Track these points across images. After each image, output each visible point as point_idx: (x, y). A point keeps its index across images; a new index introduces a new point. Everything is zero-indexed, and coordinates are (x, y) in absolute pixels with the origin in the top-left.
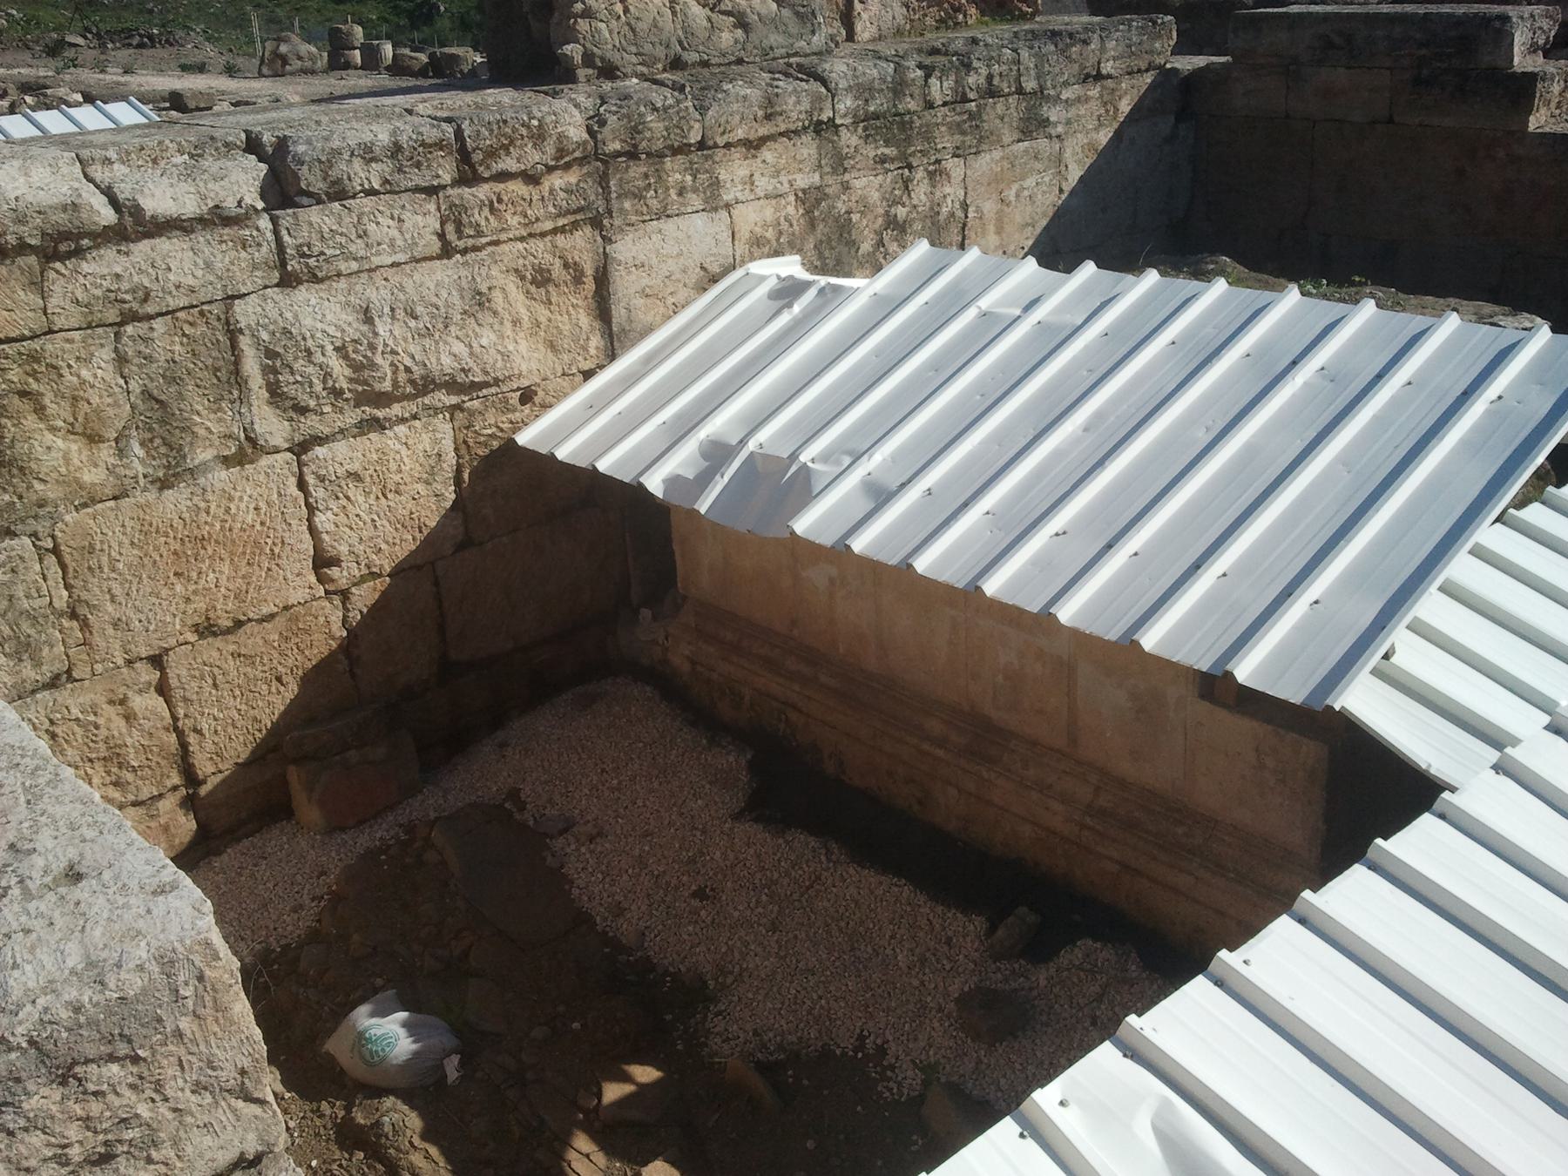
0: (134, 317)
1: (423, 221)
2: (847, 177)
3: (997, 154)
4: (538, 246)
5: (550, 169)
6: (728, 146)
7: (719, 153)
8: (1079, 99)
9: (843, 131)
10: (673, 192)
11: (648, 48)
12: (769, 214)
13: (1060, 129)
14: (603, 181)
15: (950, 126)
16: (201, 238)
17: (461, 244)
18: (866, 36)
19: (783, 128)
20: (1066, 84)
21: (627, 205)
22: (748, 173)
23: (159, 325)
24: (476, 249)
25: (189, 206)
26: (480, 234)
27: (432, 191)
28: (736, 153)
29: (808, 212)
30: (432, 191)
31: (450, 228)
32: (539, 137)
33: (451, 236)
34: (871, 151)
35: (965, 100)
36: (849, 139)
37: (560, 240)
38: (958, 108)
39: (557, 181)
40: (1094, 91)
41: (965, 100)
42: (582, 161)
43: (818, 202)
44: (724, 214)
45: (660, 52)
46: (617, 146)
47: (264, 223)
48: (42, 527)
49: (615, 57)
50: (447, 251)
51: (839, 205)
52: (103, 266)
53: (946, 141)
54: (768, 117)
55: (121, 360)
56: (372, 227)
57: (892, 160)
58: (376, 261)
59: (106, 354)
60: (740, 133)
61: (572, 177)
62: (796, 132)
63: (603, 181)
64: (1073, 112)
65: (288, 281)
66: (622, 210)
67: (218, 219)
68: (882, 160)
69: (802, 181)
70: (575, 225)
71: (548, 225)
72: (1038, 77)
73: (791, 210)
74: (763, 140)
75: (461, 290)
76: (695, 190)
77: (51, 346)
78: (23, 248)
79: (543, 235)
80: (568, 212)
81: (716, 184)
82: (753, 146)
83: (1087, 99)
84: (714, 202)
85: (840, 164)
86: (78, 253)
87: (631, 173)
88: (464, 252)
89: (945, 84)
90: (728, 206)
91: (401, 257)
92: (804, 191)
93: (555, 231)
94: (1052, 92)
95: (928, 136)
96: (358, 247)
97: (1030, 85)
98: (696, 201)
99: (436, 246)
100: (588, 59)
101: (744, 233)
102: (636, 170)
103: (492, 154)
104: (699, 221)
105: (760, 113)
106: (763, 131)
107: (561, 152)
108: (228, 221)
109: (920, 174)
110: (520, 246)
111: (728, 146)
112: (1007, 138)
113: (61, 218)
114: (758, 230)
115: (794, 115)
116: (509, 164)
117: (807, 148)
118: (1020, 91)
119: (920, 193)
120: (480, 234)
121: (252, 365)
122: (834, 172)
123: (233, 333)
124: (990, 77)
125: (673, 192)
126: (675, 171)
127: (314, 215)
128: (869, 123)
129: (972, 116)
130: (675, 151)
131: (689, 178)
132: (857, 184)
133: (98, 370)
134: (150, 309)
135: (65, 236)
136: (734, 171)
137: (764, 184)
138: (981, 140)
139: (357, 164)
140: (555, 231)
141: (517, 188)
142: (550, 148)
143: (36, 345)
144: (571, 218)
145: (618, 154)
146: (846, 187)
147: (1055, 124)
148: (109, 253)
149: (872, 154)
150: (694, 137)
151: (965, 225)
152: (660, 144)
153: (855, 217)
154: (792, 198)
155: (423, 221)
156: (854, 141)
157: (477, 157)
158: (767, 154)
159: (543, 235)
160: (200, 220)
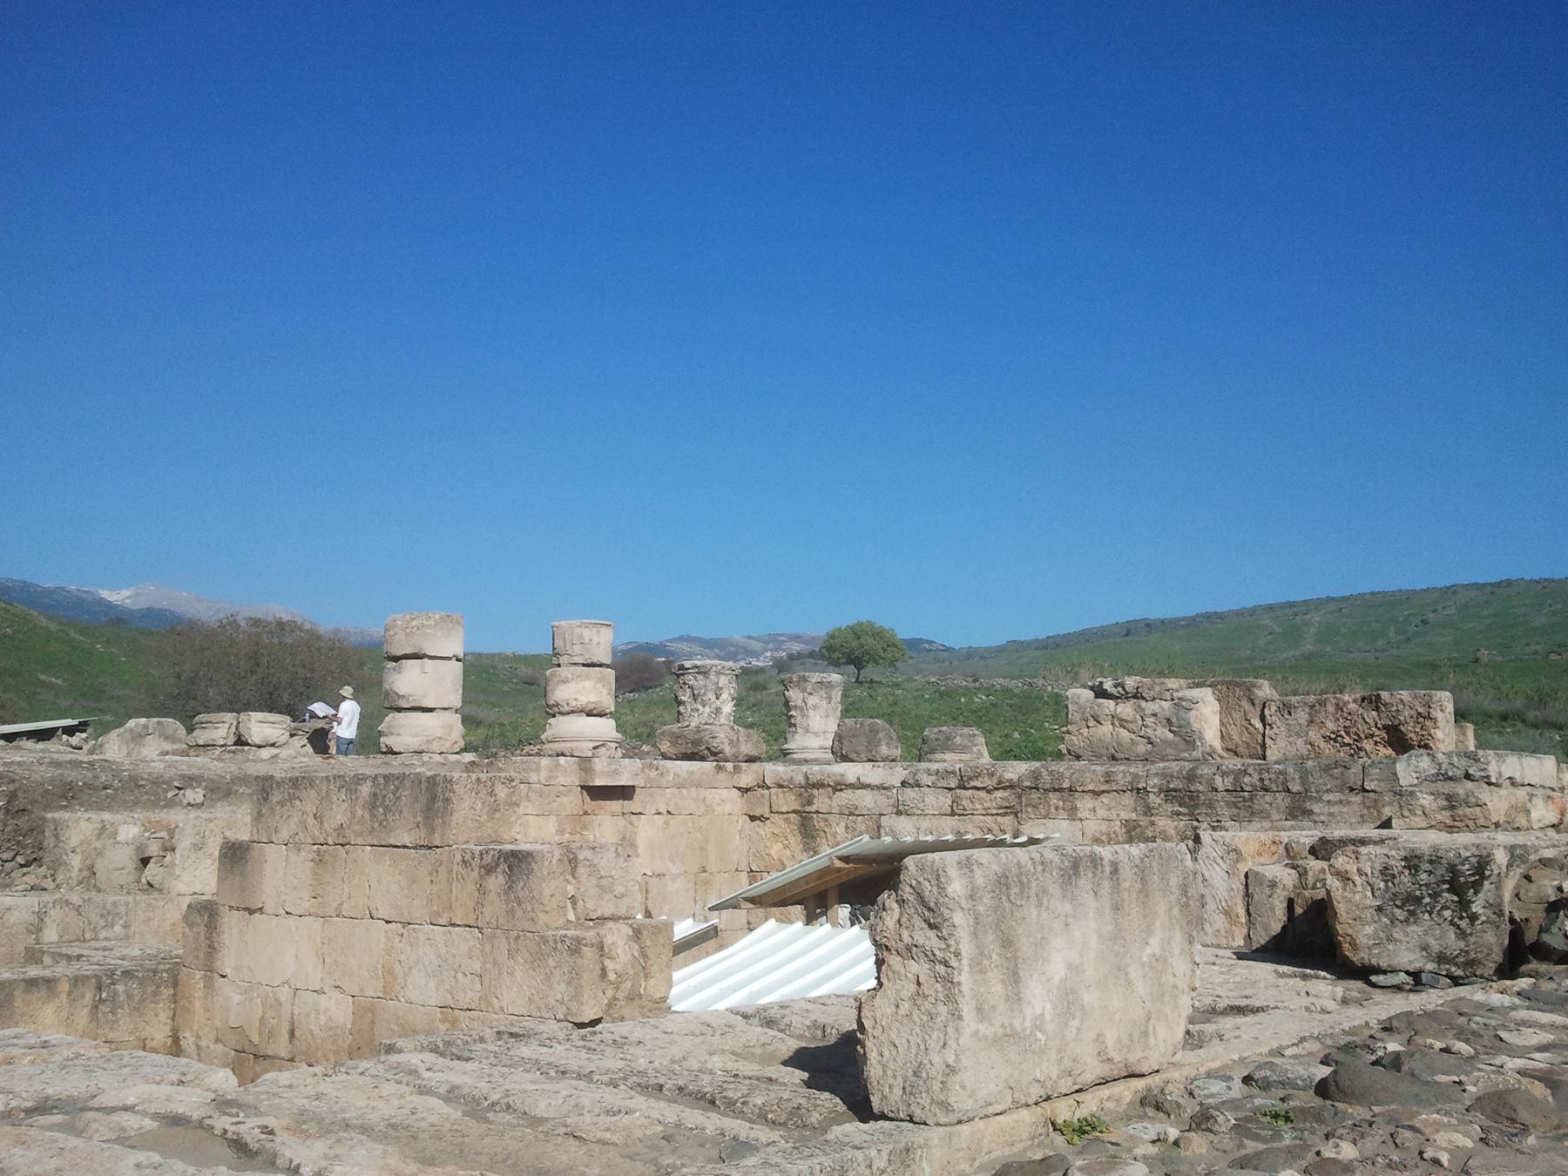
0: (851, 814)
1: (945, 800)
2: (1153, 818)
4: (988, 818)
5: (997, 789)
6: (1083, 791)
7: (1077, 795)
8: (1341, 802)
9: (1151, 795)
10: (1053, 809)
11: (1096, 749)
12: (1104, 828)
13: (1322, 818)
15: (1227, 803)
16: (875, 792)
17: (958, 812)
18: (1274, 758)
19: (1115, 788)
20: (1329, 791)
21: (1029, 809)
22: (1092, 806)
24: (963, 815)
25: (877, 782)
26: (965, 810)
27: (950, 789)
28: (1087, 797)
29: (1129, 832)
30: (950, 789)
31: (955, 805)
32: (992, 775)
33: (955, 808)
34: (1169, 808)
35: (1243, 791)
36: (1154, 800)
37: (999, 818)
38: (1234, 794)
39: (999, 794)
40: (1356, 799)
41: (1243, 791)
42: (1012, 787)
43: (1135, 828)
45: (1104, 752)
46: (1029, 784)
47: (895, 791)
49: (1081, 753)
50: (953, 814)
51: (1148, 832)
53: (1225, 812)
54: (1107, 782)
55: (847, 828)
56: (926, 799)
57: (1185, 815)
58: (927, 812)
59: (843, 824)
60: (1090, 787)
61: (1006, 794)
62: (1124, 791)
63: (1020, 797)
64: (1335, 809)
65: (899, 813)
66: (1027, 811)
68: (1178, 814)
69: (1124, 815)
70: (1006, 814)
71: (995, 812)
72: (1303, 784)
73: (1117, 829)
74: (1103, 792)
76: (1064, 809)
78: (829, 785)
79: (992, 815)
80: (1001, 808)
81: (1074, 809)
82: (1097, 794)
83: (1349, 803)
85: (1148, 811)
86: (841, 790)
87: (1032, 796)
88: (959, 815)
90: (1081, 820)
91: (936, 813)
93: (997, 814)
94: (1314, 795)
95: (1211, 805)
96: (921, 806)
97: (1295, 788)
98: (1065, 815)
99: (949, 811)
100: (1069, 751)
101: (1089, 833)
102: (1035, 795)
103: (971, 779)
104: (1065, 823)
105: (1102, 779)
106: (1103, 788)
107: (1000, 782)
108: (885, 788)
109: (1205, 825)
110: (982, 817)
111: (1083, 791)
112: (1275, 816)
113: (838, 778)
115: (1122, 783)
116: (977, 783)
117: (1128, 799)
118: (1288, 791)
120: (965, 810)
122: (1145, 814)
123: (879, 827)
124: (1261, 780)
125: (1053, 809)
126: (1054, 799)
127: (908, 791)
128: (1168, 794)
129: (1245, 800)
130: (1055, 790)
131: (1061, 803)
132: (1160, 823)
134: (857, 813)
135: (839, 784)
136: (1085, 804)
137: (1101, 813)
138: (1253, 814)
139: (925, 775)
140: (997, 814)
141: (983, 794)
142: (995, 780)
143: (827, 816)
144: (1004, 810)
145: (1031, 788)
146: (1152, 824)
147: (1319, 815)
148: (849, 791)
149: (1170, 809)
152: (1048, 786)
155: (945, 800)
156: (1158, 801)
157: (965, 779)
158: (1104, 799)
159: (992, 815)
160: (876, 786)
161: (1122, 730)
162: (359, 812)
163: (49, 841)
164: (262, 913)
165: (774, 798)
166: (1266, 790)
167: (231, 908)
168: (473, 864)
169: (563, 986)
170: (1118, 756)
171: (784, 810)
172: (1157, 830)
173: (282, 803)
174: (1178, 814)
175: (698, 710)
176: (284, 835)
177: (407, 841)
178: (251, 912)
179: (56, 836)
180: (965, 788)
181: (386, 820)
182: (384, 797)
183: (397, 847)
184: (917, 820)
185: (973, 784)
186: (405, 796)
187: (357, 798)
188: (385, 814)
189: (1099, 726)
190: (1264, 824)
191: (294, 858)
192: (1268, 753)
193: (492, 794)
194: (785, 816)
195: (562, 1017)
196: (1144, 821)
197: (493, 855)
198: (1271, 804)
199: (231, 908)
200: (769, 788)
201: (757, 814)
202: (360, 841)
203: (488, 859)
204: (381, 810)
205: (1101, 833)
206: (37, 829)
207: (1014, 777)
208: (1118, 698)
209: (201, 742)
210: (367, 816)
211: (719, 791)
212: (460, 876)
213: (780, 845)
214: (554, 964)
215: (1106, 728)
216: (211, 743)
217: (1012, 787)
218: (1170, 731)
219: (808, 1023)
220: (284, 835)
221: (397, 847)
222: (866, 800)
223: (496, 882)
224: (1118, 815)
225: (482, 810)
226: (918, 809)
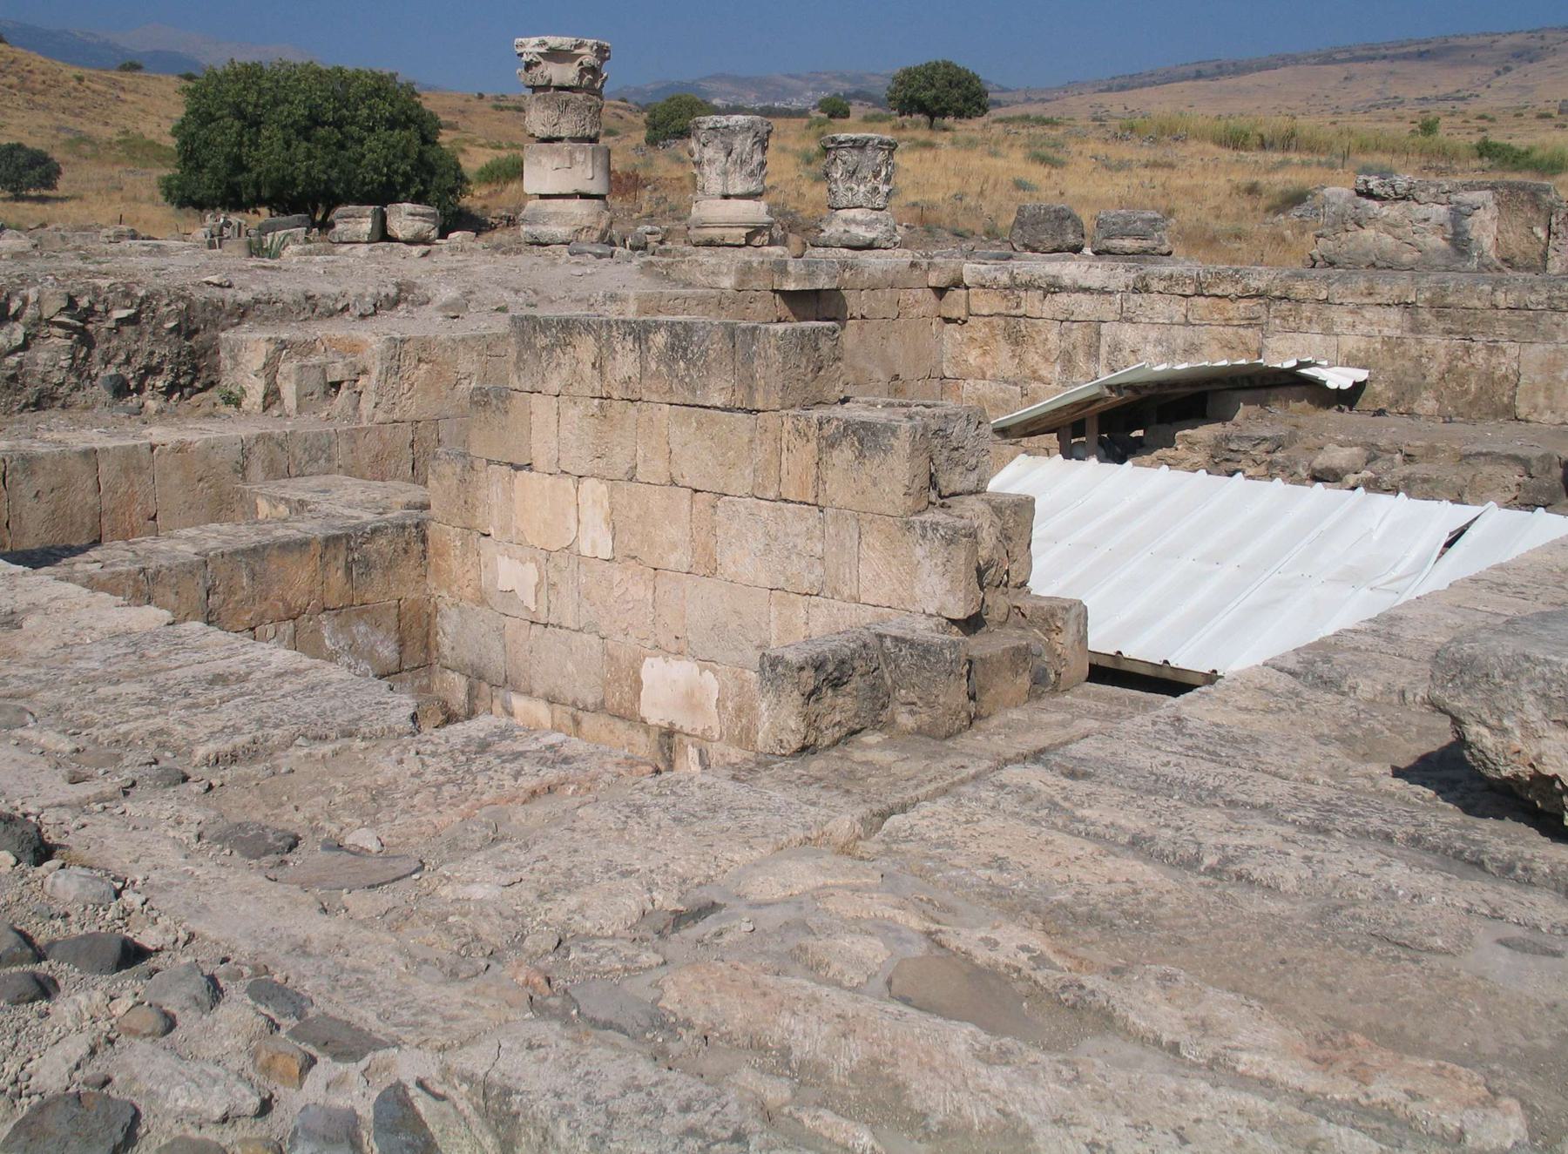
0: (1067, 320)
3: (1551, 347)
4: (1230, 330)
12: (1363, 345)
14: (1268, 307)
15: (1510, 324)
18: (1556, 271)
21: (1277, 321)
23: (1075, 325)
25: (1097, 285)
26: (1201, 319)
36: (1426, 315)
37: (1241, 331)
39: (1243, 304)
42: (1259, 296)
44: (1335, 338)
47: (1118, 296)
48: (1026, 386)
52: (1062, 298)
57: (1458, 333)
58: (1156, 320)
59: (1056, 330)
63: (1268, 307)
67: (1103, 291)
69: (1387, 332)
71: (1235, 323)
73: (1378, 346)
75: (1186, 341)
77: (1040, 322)
78: (1039, 288)
84: (1327, 331)
85: (1417, 328)
86: (1055, 292)
89: (1509, 297)
92: (1389, 338)
93: (1239, 326)
98: (1317, 329)
99: (1183, 320)
101: (1345, 349)
102: (1285, 306)
104: (1318, 338)
114: (1354, 351)
117: (1395, 315)
119: (1479, 358)
121: (1104, 350)
122: (1412, 330)
123: (1099, 334)
132: (1427, 341)
133: (1053, 337)
134: (1073, 318)
135: (1053, 286)
137: (1362, 328)
140: (1239, 326)
146: (1419, 342)
148: (1064, 295)
150: (1323, 296)
151: (1516, 385)
153: (1424, 360)
154: (1379, 339)
156: (1428, 317)
161: (1385, 235)
162: (653, 366)
163: (226, 363)
164: (531, 470)
165: (973, 301)
166: (1554, 309)
167: (489, 462)
168: (810, 434)
169: (935, 579)
170: (1379, 264)
171: (985, 312)
172: (1424, 348)
173: (550, 349)
174: (1449, 332)
175: (852, 189)
176: (555, 384)
177: (718, 400)
178: (518, 468)
179: (234, 358)
180: (1202, 295)
181: (689, 375)
182: (685, 349)
183: (708, 408)
184: (1144, 330)
185: (1213, 291)
186: (715, 350)
187: (649, 349)
188: (688, 369)
189: (1360, 230)
190: (1548, 346)
191: (573, 413)
192: (1550, 264)
193: (817, 349)
194: (987, 319)
195: (934, 612)
196: (1410, 340)
197: (837, 427)
198: (1558, 325)
199: (489, 462)
200: (967, 288)
201: (954, 315)
202: (655, 398)
203: (829, 430)
204: (681, 363)
205: (1359, 350)
206: (212, 349)
207: (1262, 285)
208: (1384, 199)
209: (344, 239)
210: (663, 369)
211: (913, 291)
212: (791, 447)
213: (979, 351)
214: (923, 553)
215: (1369, 233)
216: (355, 239)
217: (1259, 296)
218: (1444, 239)
219: (1379, 687)
220: (555, 384)
221: (708, 408)
222: (1085, 306)
223: (844, 455)
224: (1380, 331)
225: (806, 368)
226: (1146, 316)
